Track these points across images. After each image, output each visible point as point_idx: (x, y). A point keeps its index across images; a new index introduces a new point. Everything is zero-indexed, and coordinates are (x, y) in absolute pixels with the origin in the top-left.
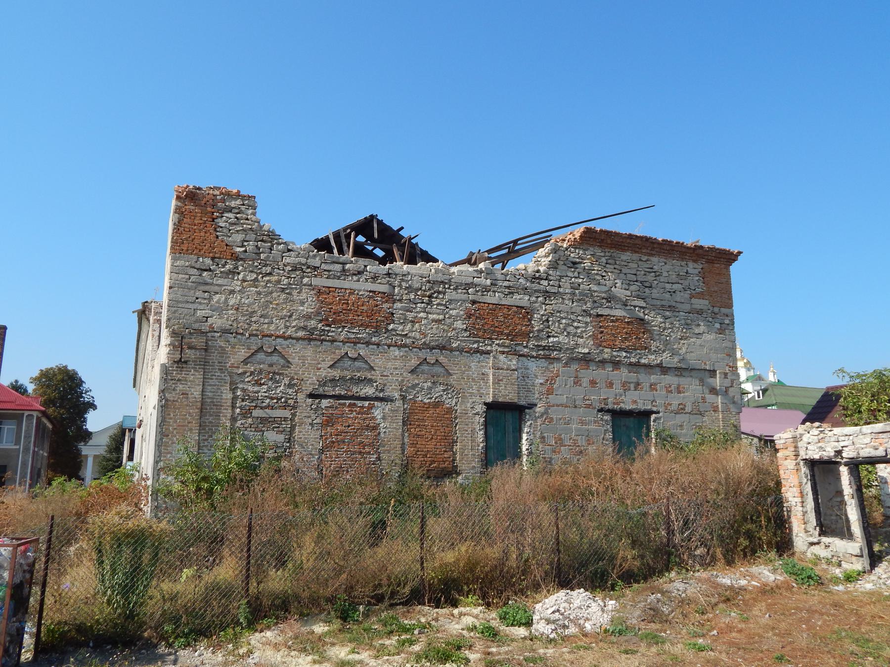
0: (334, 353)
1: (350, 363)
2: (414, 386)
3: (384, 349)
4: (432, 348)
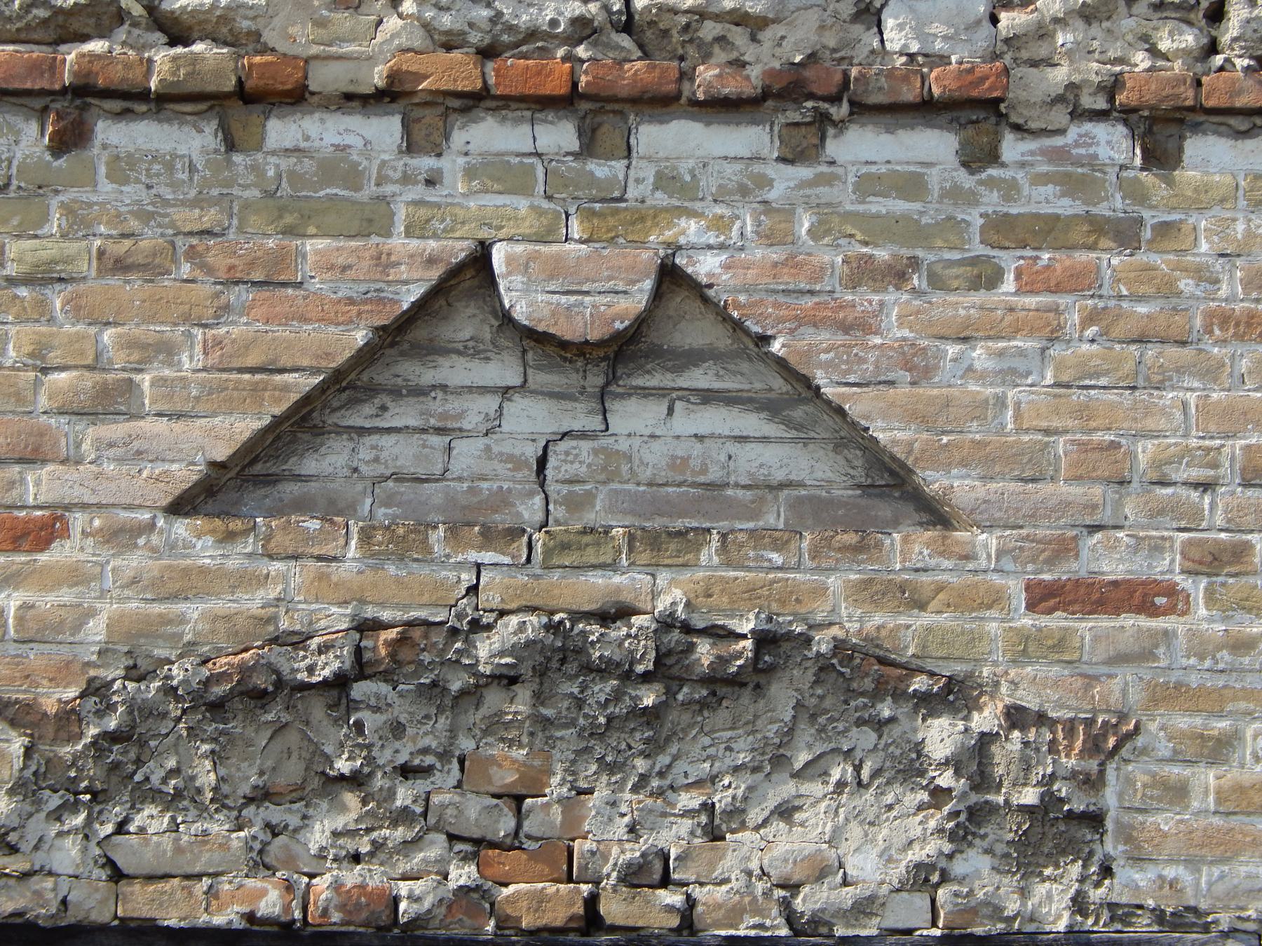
0: (274, 279)
1: (530, 419)
3: (1079, 178)
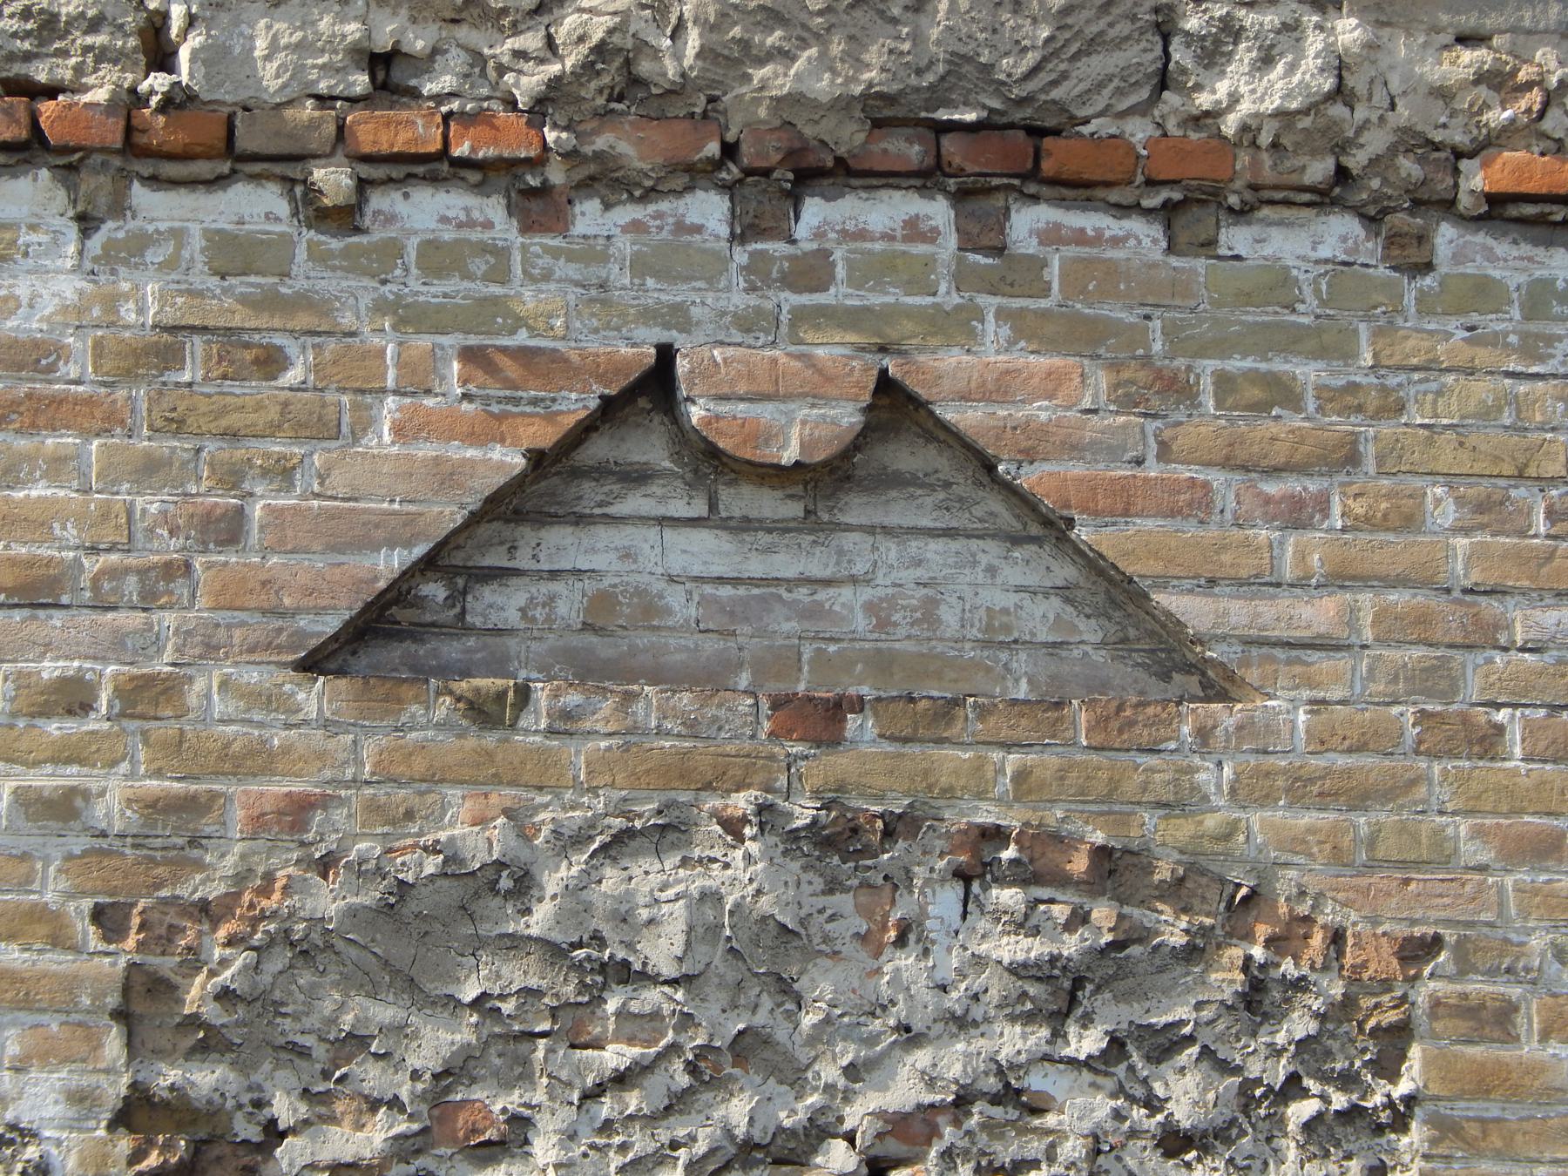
2: (425, 923)
4: (786, 173)
